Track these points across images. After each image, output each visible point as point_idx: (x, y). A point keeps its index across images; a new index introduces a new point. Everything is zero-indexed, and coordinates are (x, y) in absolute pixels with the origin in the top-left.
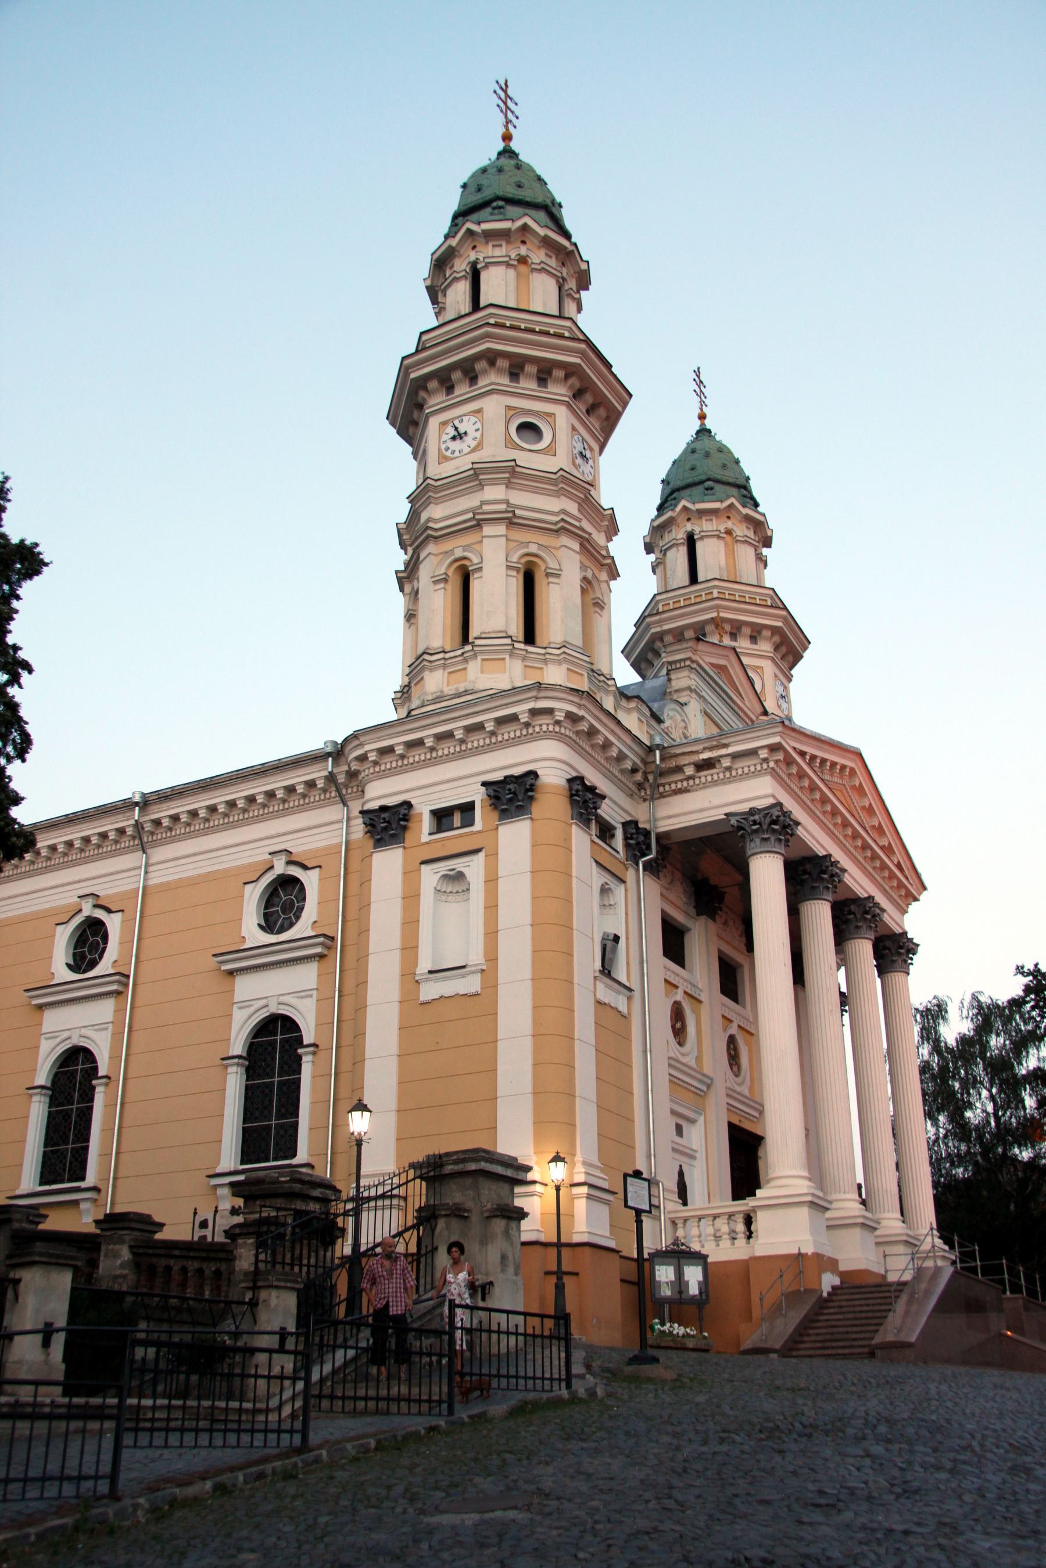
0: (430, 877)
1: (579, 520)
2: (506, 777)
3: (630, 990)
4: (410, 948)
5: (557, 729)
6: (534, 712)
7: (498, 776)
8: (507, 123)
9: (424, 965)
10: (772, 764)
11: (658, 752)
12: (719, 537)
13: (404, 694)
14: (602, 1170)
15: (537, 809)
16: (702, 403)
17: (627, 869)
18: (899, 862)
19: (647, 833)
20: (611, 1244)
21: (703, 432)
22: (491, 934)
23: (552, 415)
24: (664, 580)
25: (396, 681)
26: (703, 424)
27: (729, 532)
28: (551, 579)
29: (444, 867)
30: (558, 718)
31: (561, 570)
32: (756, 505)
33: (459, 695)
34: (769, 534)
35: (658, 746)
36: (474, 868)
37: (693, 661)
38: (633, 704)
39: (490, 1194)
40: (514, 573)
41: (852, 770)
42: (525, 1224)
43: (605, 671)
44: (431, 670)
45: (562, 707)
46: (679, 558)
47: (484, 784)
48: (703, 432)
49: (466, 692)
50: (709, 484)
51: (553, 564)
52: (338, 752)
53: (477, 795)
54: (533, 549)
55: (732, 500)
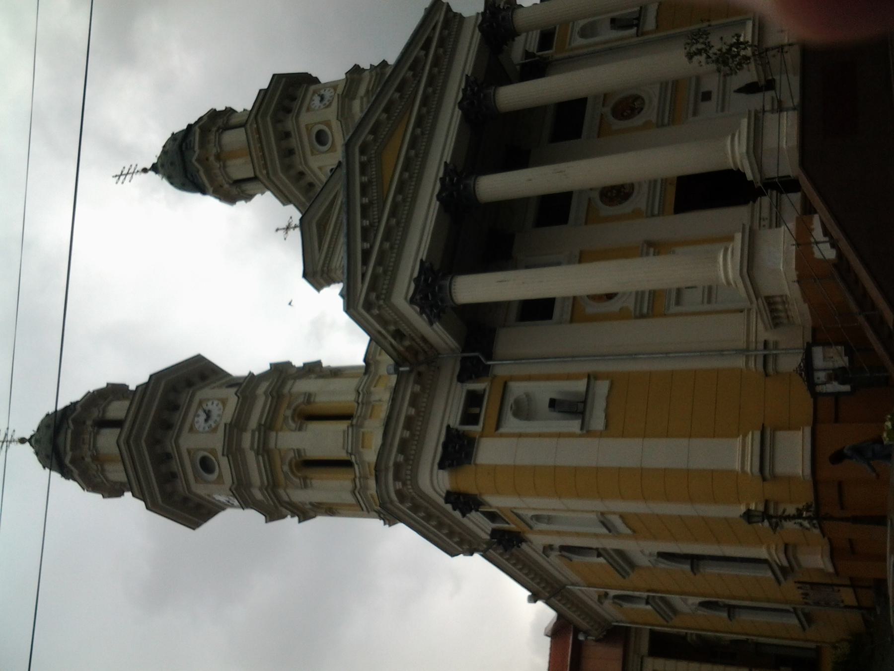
1: (253, 432)
3: (589, 377)
4: (596, 535)
5: (409, 482)
8: (14, 441)
10: (381, 302)
11: (402, 369)
12: (225, 167)
14: (745, 436)
15: (473, 490)
17: (495, 376)
18: (422, 48)
19: (464, 360)
20: (808, 430)
21: (155, 168)
23: (189, 452)
26: (150, 169)
27: (218, 157)
28: (303, 454)
29: (532, 523)
30: (401, 487)
31: (294, 450)
32: (190, 127)
34: (205, 119)
35: (396, 371)
37: (323, 271)
38: (371, 362)
40: (308, 481)
41: (363, 151)
45: (392, 486)
46: (249, 187)
47: (464, 515)
48: (155, 168)
50: (189, 176)
51: (292, 454)
54: (286, 468)
55: (194, 160)
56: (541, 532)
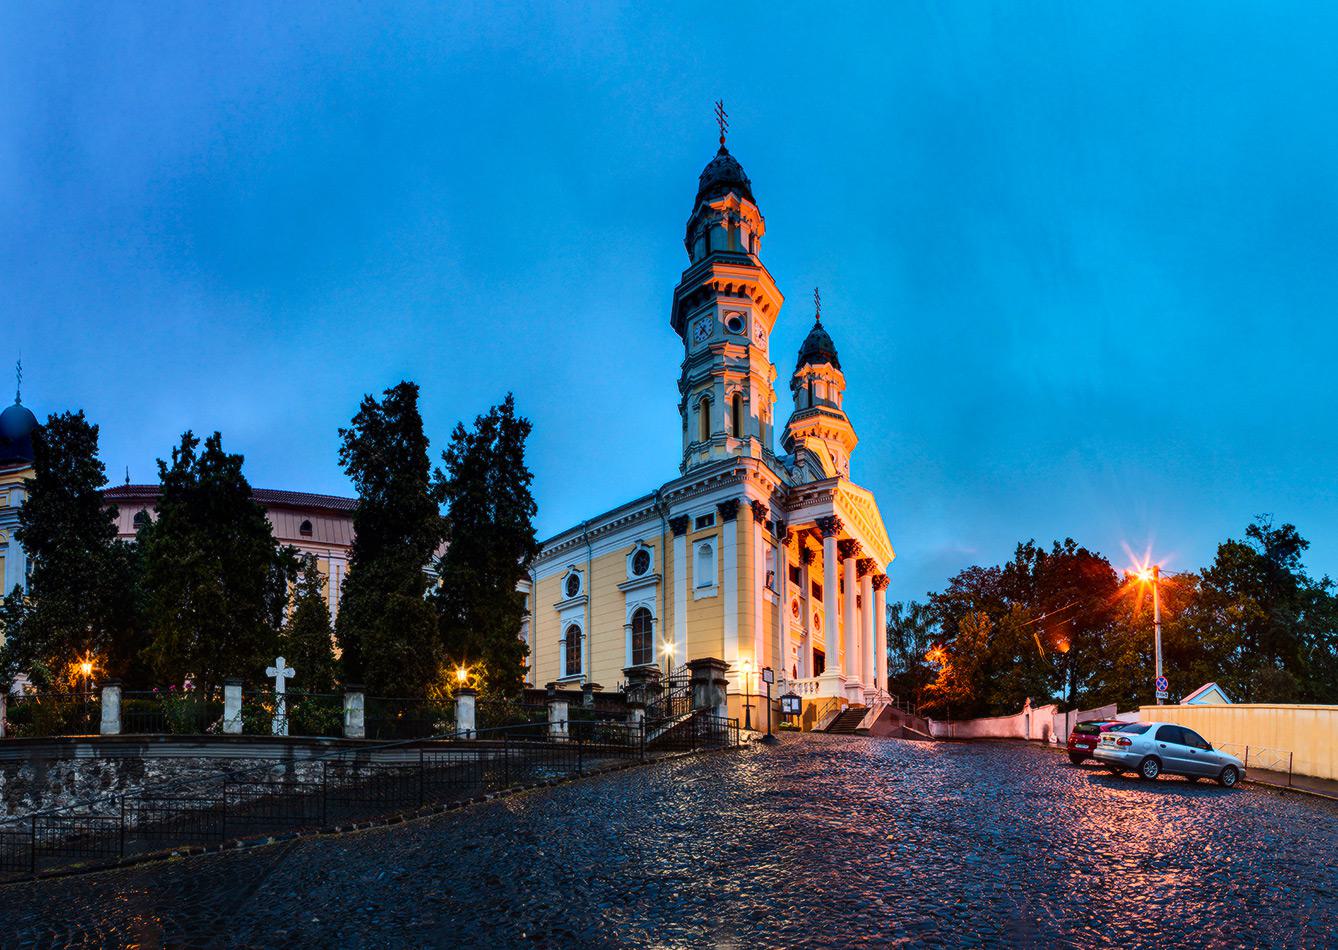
0: (697, 548)
2: (728, 502)
6: (738, 471)
7: (723, 501)
9: (696, 585)
13: (683, 467)
15: (739, 517)
16: (818, 309)
22: (721, 571)
24: (798, 405)
25: (680, 459)
33: (705, 464)
36: (714, 544)
39: (714, 675)
42: (728, 687)
43: (770, 449)
44: (695, 453)
49: (709, 462)
52: (658, 495)
53: (713, 510)
56: (689, 547)
